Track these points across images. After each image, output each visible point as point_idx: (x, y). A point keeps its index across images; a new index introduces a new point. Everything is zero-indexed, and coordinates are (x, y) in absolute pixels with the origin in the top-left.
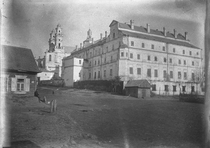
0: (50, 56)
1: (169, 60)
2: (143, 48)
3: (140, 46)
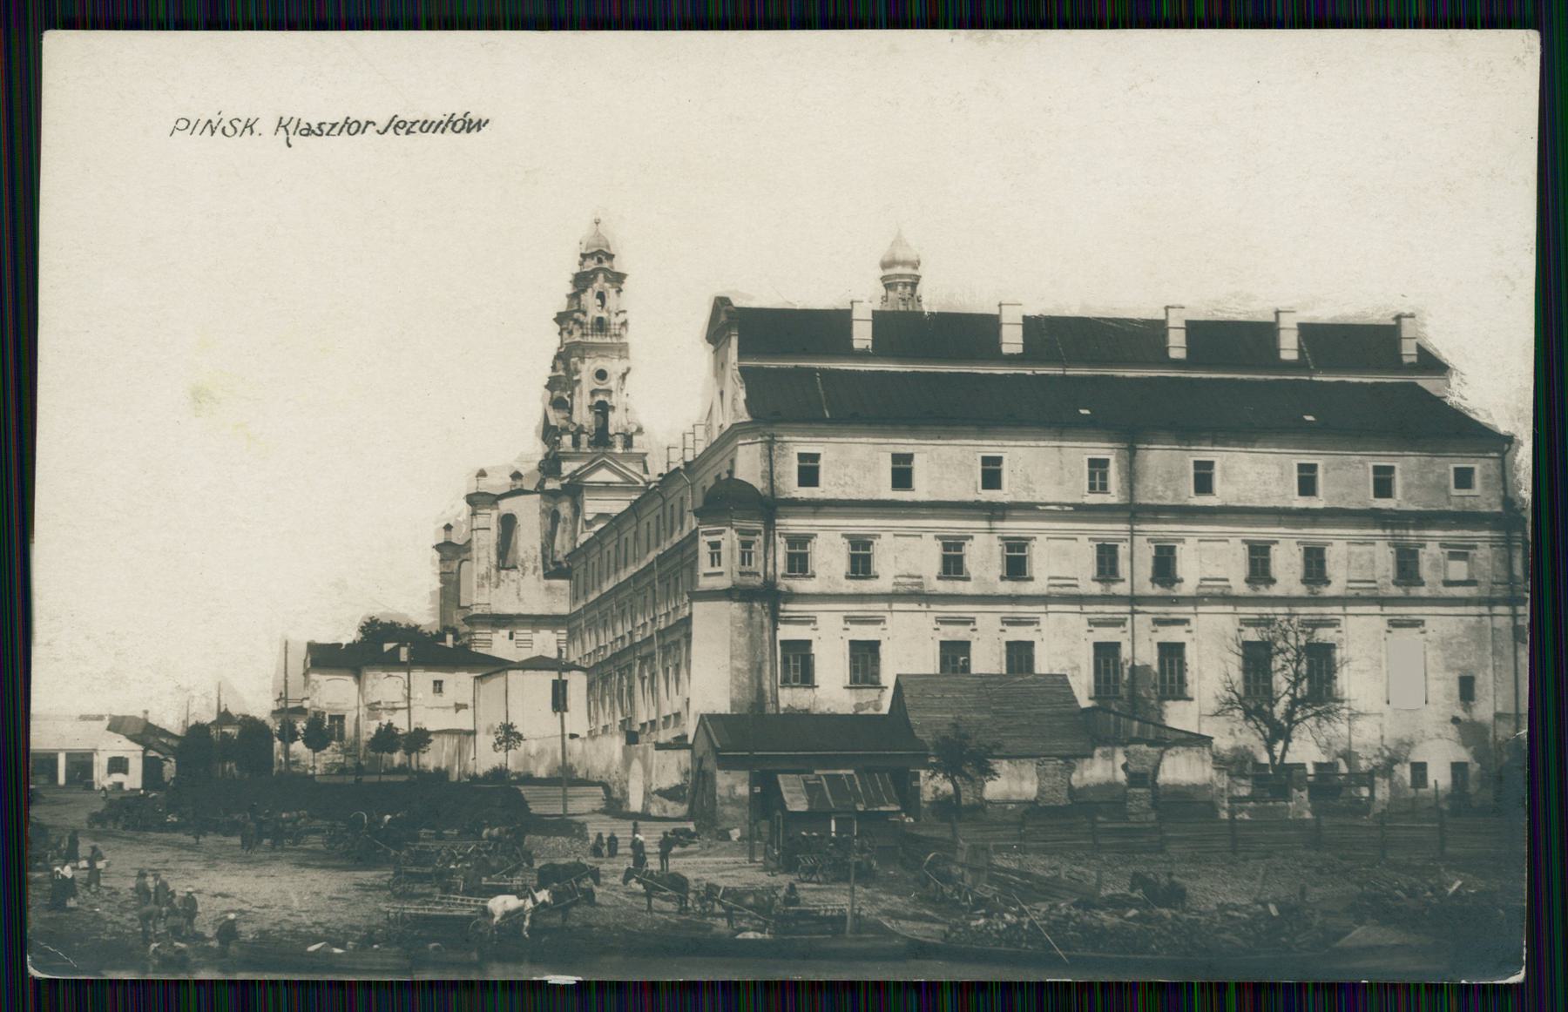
0: (508, 522)
1: (1145, 569)
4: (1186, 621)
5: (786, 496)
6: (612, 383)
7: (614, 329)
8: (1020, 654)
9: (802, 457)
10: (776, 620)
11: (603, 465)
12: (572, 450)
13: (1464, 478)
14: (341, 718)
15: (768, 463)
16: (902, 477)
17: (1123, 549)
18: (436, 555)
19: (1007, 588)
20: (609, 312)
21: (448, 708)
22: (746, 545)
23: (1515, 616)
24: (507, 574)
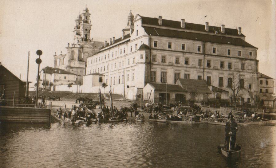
0: (73, 52)
1: (206, 65)
2: (170, 49)
4: (211, 73)
6: (88, 31)
7: (89, 23)
8: (187, 76)
9: (155, 41)
11: (87, 44)
13: (251, 54)
14: (48, 82)
16: (170, 46)
17: (203, 61)
18: (54, 57)
19: (185, 65)
21: (67, 81)
23: (257, 76)
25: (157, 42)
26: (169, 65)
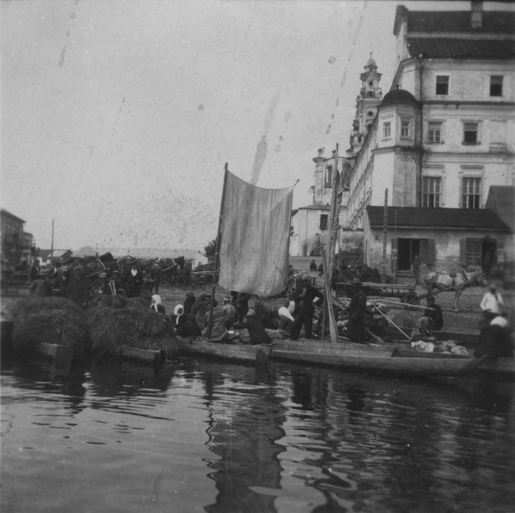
2: (498, 99)
3: (485, 95)
5: (429, 99)
9: (438, 77)
10: (421, 166)
12: (358, 143)
15: (419, 81)
20: (374, 89)
22: (405, 124)
24: (329, 190)
25: (446, 78)
26: (491, 154)
